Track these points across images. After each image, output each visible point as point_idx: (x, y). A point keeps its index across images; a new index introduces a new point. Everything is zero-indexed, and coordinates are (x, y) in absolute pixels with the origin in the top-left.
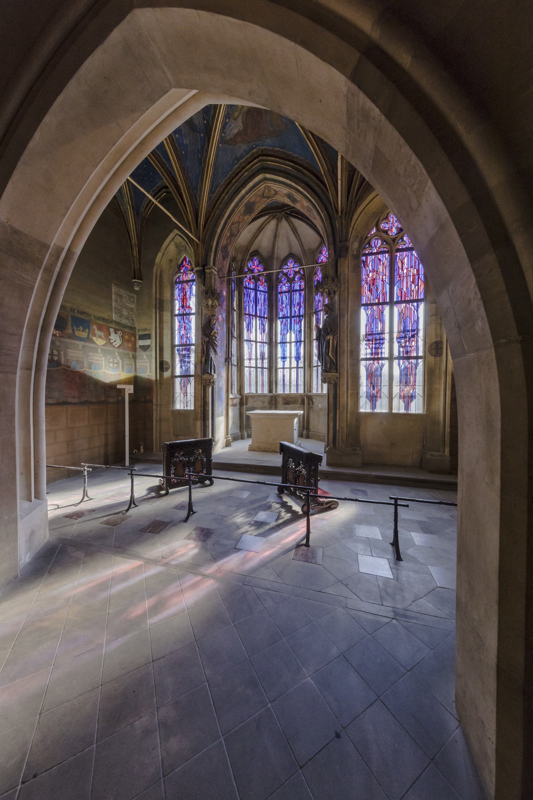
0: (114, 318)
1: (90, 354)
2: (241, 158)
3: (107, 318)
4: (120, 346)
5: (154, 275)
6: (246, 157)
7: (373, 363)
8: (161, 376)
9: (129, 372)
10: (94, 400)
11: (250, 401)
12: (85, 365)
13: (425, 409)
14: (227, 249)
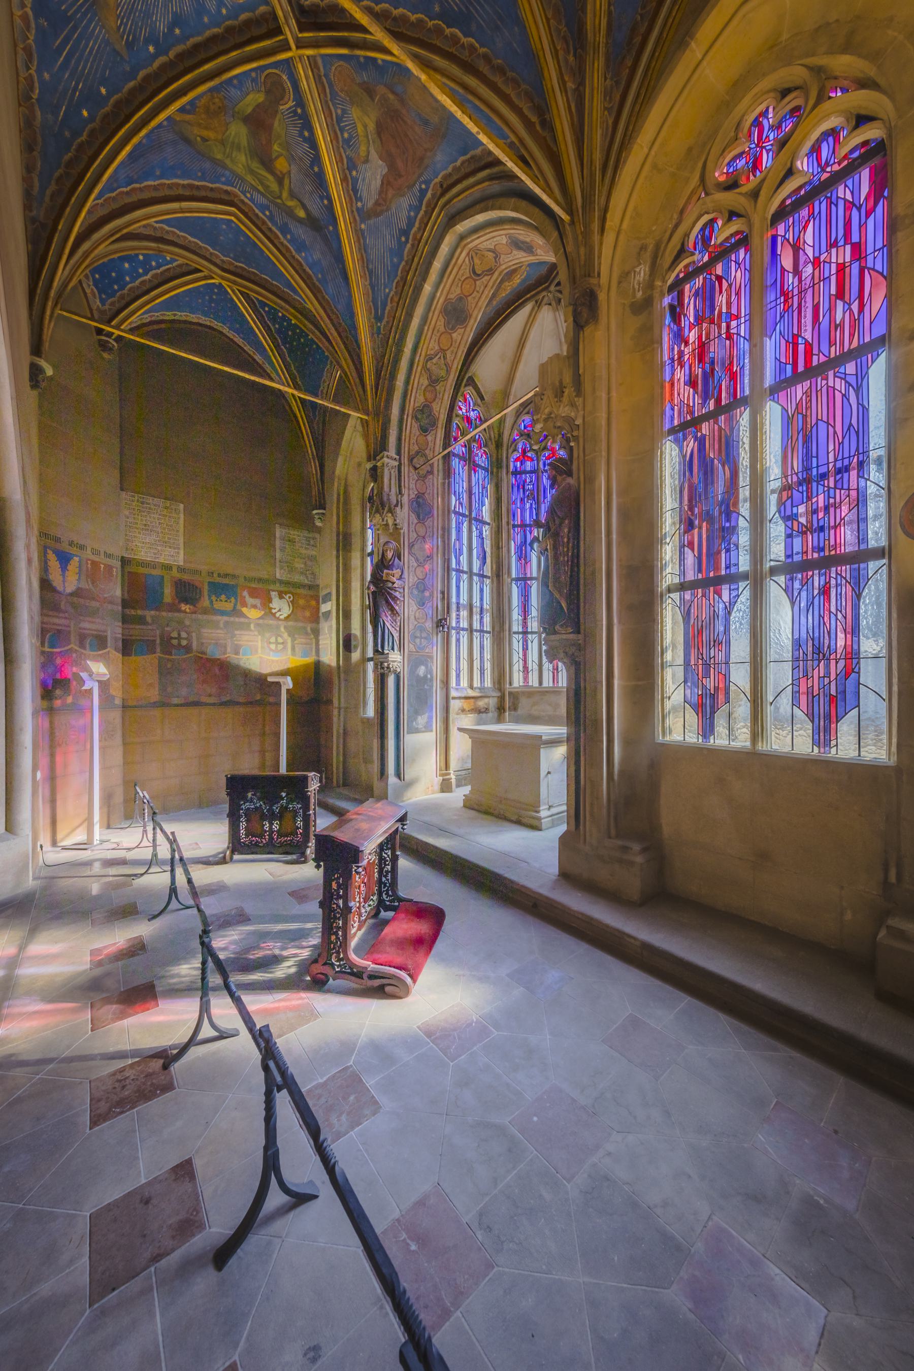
0: (278, 576)
1: (237, 632)
2: (411, 224)
3: (267, 577)
4: (289, 616)
5: (335, 496)
6: (420, 216)
7: (704, 595)
8: (347, 659)
9: (305, 655)
10: (241, 700)
11: (524, 702)
12: (229, 650)
13: (894, 749)
14: (431, 410)
